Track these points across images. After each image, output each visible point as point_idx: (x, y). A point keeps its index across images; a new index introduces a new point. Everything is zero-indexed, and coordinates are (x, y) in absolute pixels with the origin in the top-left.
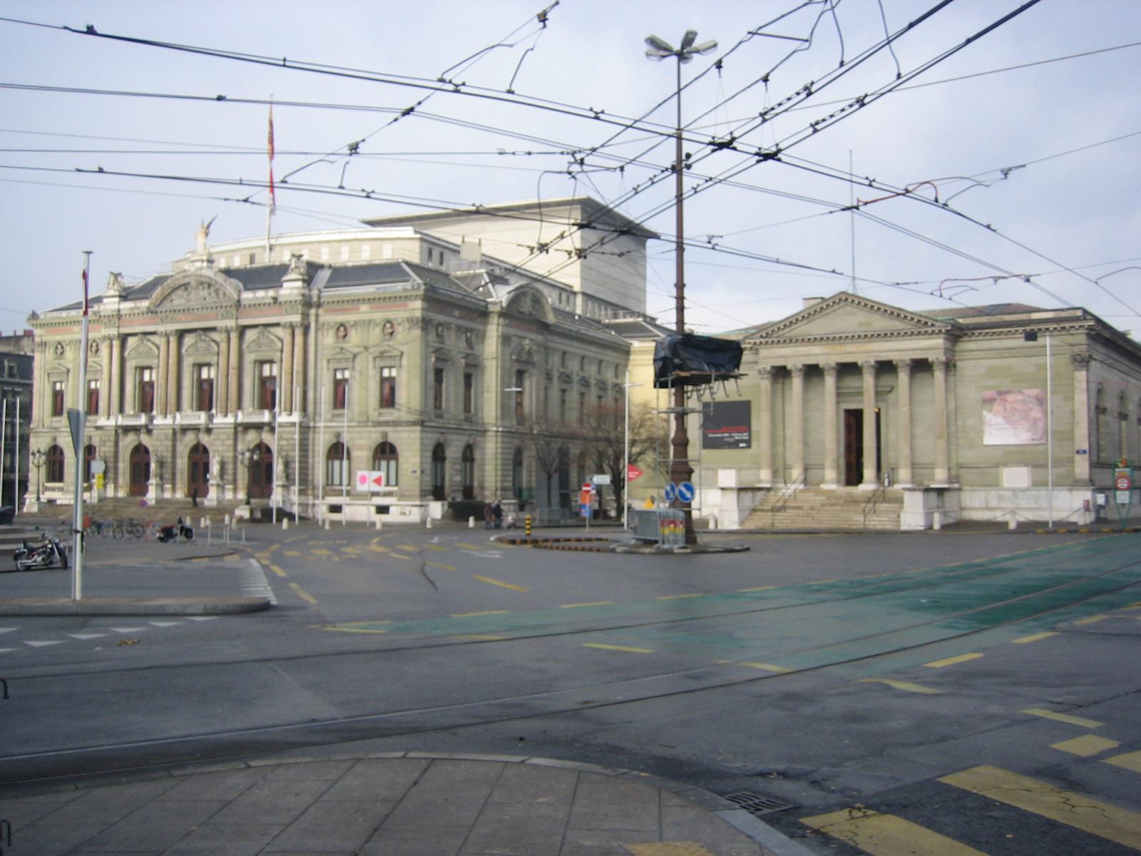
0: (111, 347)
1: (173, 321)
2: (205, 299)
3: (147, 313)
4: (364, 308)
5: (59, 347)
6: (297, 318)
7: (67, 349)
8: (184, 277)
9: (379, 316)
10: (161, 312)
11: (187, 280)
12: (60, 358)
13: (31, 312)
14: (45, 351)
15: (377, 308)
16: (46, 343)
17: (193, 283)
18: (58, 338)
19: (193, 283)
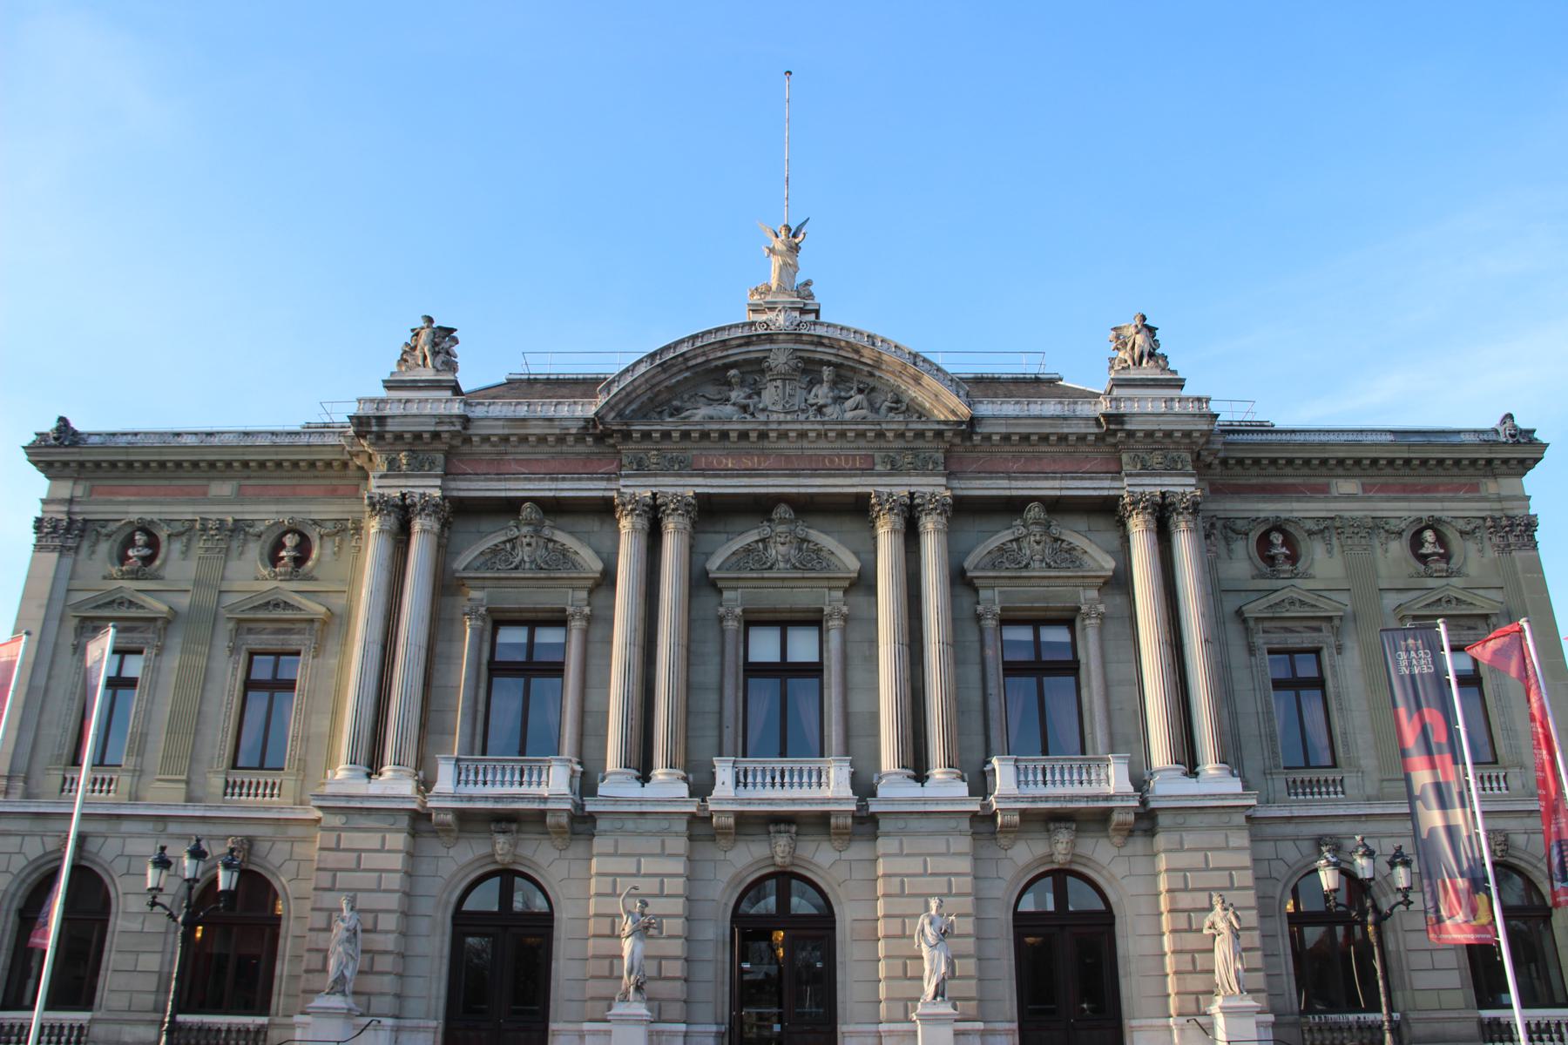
0: (401, 537)
1: (684, 467)
2: (820, 410)
3: (580, 439)
4: (1348, 486)
5: (140, 538)
6: (1183, 486)
7: (172, 551)
8: (748, 341)
9: (1403, 510)
10: (646, 435)
11: (754, 351)
12: (135, 575)
13: (49, 425)
14: (77, 549)
15: (1384, 488)
16: (85, 521)
17: (780, 358)
18: (137, 512)
19: (780, 358)
